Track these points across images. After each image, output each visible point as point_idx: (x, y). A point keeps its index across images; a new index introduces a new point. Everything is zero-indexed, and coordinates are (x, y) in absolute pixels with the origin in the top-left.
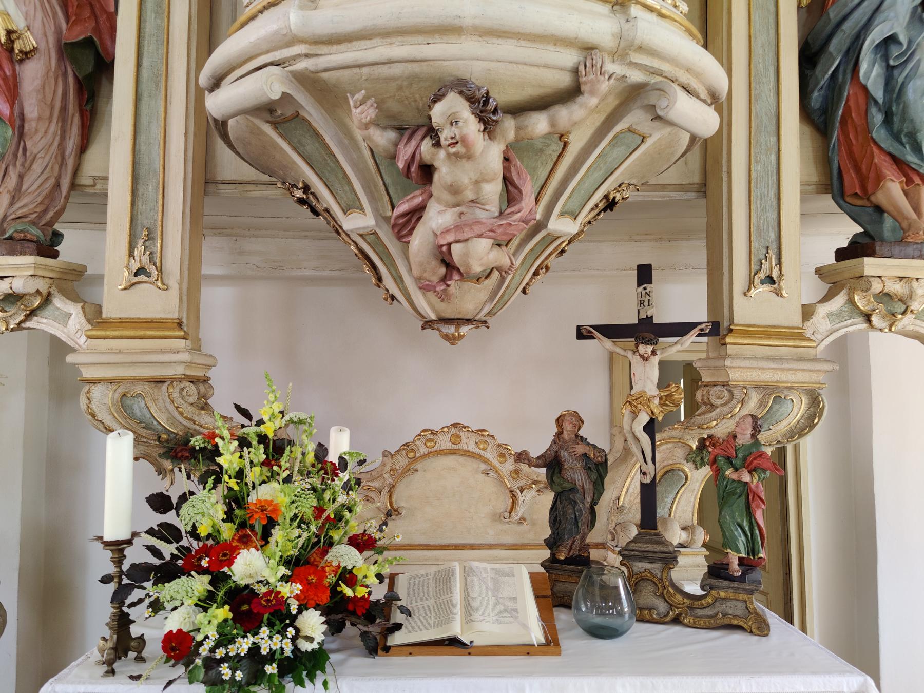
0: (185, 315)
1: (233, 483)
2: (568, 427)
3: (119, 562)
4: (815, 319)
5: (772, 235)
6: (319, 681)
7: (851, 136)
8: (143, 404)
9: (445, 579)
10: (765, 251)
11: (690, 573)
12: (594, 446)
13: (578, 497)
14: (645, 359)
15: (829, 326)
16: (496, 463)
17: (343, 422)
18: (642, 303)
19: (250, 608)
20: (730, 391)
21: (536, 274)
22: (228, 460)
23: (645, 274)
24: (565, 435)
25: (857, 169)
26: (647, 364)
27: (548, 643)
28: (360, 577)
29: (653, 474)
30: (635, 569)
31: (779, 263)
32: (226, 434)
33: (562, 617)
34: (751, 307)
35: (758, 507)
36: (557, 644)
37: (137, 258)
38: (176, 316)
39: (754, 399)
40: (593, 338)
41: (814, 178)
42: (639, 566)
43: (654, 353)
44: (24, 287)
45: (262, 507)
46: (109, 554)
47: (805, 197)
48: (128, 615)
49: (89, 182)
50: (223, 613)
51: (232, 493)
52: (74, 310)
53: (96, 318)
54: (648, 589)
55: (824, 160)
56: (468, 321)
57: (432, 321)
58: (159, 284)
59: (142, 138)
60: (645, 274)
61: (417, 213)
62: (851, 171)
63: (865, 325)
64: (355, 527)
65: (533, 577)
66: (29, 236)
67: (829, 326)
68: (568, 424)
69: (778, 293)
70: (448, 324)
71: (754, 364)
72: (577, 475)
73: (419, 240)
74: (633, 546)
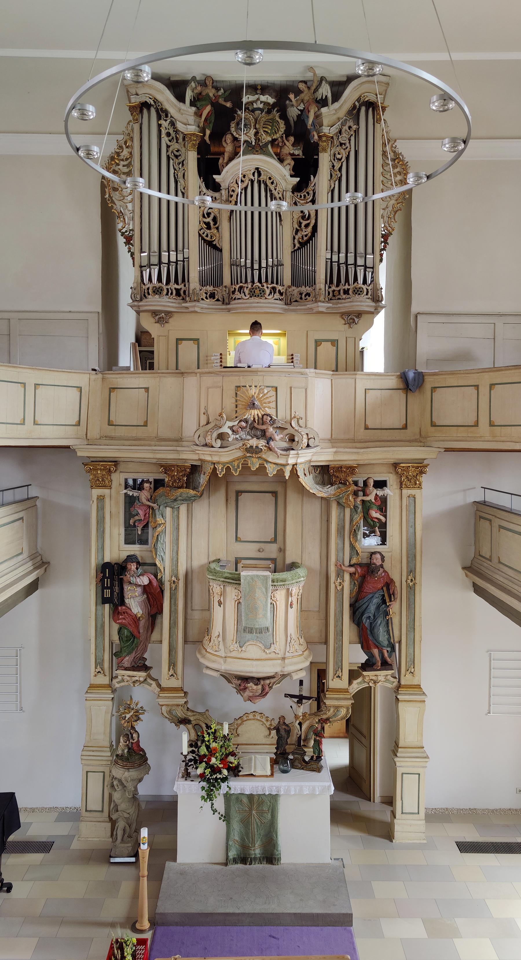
16: (265, 722)
31: (342, 672)
39: (332, 710)
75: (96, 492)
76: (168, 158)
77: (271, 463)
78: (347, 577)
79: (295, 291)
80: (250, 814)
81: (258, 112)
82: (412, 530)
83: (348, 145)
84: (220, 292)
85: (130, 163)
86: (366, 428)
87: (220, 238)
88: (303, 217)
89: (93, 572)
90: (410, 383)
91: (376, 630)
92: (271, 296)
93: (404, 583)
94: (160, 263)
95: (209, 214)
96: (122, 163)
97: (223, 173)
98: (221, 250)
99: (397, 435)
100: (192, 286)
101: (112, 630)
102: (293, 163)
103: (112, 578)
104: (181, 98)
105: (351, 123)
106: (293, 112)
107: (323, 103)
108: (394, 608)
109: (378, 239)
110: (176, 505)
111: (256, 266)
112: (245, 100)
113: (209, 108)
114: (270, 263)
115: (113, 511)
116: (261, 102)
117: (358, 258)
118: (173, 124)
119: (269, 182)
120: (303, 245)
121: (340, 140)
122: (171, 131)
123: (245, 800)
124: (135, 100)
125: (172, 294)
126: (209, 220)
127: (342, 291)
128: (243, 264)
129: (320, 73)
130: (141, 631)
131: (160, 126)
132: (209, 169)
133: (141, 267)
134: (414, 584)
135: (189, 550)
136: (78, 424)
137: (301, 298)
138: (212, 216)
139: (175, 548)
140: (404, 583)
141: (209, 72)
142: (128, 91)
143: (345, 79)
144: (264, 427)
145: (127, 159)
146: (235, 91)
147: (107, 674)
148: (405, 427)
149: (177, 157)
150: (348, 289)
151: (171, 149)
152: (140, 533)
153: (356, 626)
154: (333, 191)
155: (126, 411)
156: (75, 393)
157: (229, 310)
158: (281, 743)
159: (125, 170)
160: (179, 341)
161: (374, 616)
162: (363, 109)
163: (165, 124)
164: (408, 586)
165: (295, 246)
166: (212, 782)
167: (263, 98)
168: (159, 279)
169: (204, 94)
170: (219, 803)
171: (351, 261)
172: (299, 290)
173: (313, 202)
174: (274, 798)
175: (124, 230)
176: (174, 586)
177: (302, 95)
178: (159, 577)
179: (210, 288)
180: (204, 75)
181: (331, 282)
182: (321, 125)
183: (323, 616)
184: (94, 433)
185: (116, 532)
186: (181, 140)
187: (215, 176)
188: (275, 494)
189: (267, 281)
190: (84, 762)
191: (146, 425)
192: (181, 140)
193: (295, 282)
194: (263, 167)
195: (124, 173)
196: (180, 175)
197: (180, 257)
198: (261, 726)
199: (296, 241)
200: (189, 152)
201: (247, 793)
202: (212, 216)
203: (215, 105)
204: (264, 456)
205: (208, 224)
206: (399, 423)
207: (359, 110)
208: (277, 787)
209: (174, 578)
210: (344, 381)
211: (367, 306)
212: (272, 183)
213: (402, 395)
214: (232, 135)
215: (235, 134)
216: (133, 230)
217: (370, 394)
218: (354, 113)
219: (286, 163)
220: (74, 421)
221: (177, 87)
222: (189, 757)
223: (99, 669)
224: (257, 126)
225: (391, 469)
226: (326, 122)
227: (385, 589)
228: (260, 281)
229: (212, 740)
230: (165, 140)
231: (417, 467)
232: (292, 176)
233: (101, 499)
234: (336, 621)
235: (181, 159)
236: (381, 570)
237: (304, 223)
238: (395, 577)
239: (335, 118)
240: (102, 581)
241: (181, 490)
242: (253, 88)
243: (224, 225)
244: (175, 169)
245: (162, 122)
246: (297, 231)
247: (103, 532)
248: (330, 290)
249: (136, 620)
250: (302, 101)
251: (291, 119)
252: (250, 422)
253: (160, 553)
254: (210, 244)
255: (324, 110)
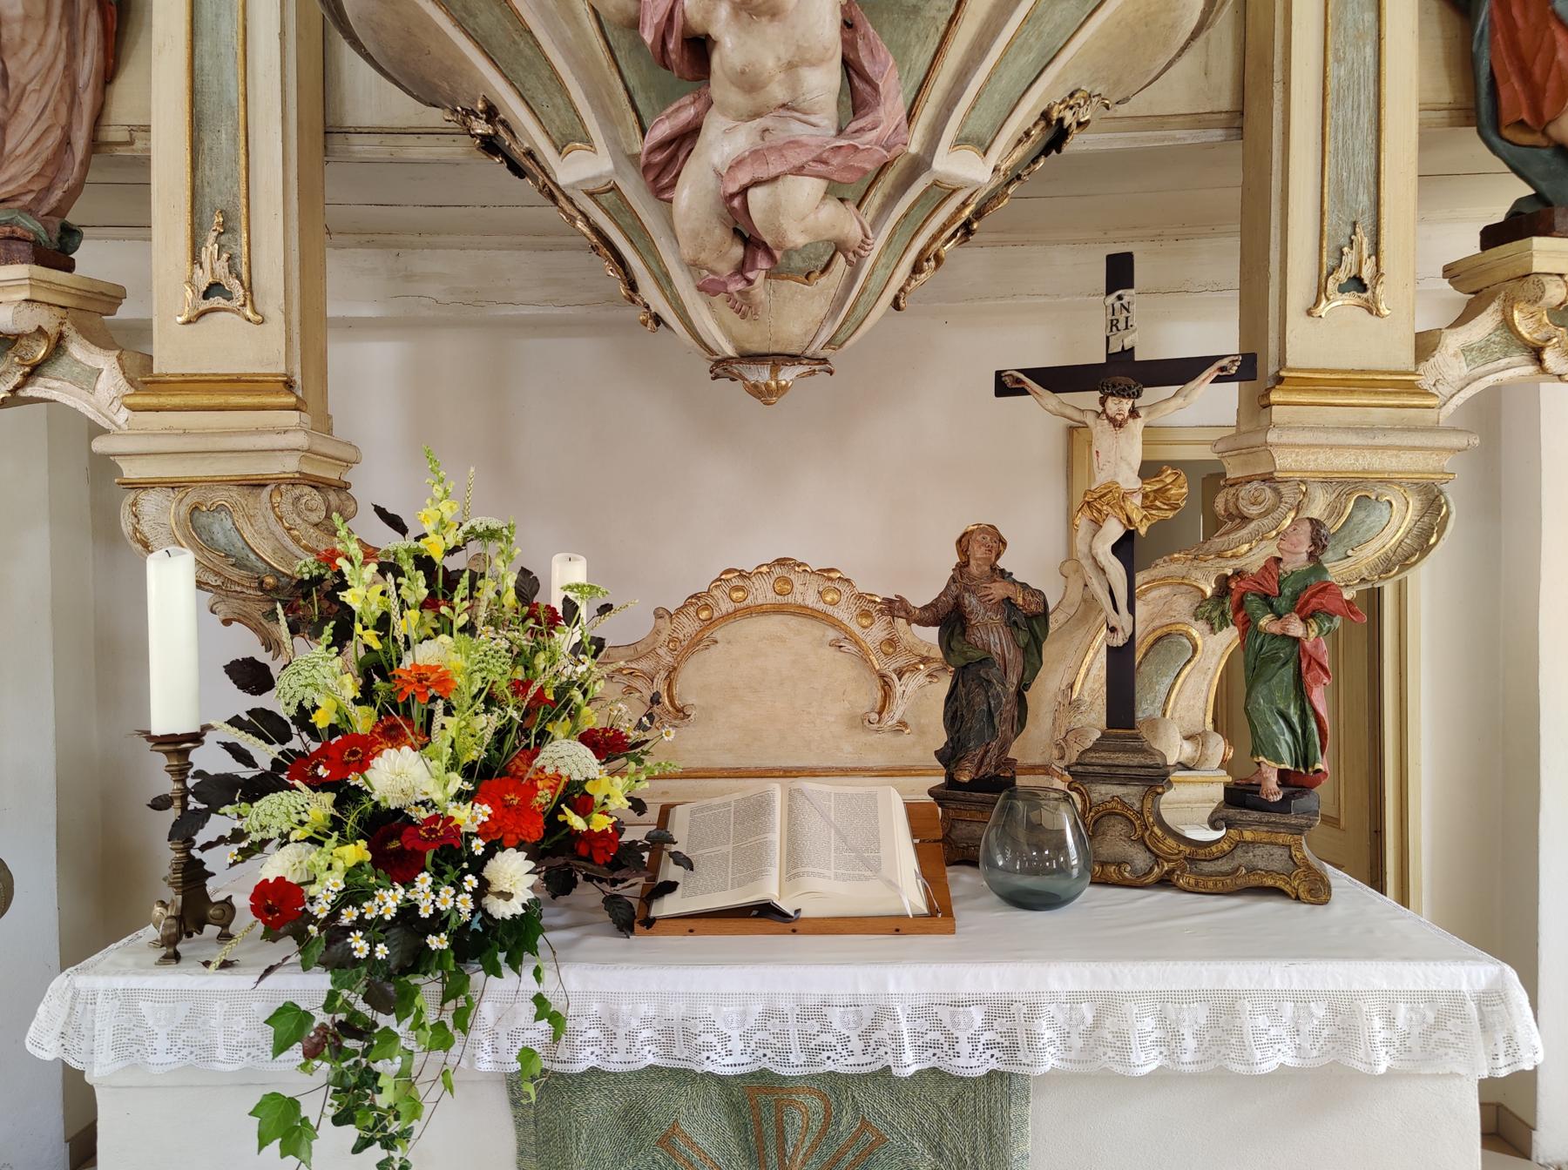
0: (297, 369)
1: (370, 637)
2: (977, 552)
3: (180, 773)
4: (1438, 358)
5: (1365, 200)
6: (527, 971)
7: (1516, 12)
8: (228, 524)
9: (757, 811)
10: (1349, 230)
11: (1191, 807)
12: (1025, 586)
13: (994, 674)
14: (1117, 424)
15: (1465, 371)
16: (854, 627)
17: (573, 547)
18: (1113, 324)
19: (396, 841)
20: (1277, 491)
21: (917, 269)
22: (363, 593)
23: (1120, 272)
24: (973, 568)
25: (1525, 74)
26: (1122, 433)
27: (933, 913)
28: (598, 798)
29: (1129, 632)
30: (1095, 797)
32: (354, 549)
33: (962, 880)
34: (1319, 335)
35: (1317, 681)
36: (948, 914)
37: (207, 265)
38: (282, 369)
40: (1023, 392)
41: (1446, 97)
42: (1103, 792)
43: (1134, 413)
44: (14, 322)
45: (421, 676)
46: (162, 760)
47: (1426, 142)
48: (201, 863)
49: (121, 136)
50: (357, 852)
51: (372, 656)
52: (105, 362)
53: (144, 379)
54: (1117, 828)
55: (1464, 61)
56: (794, 358)
57: (727, 360)
58: (249, 313)
59: (205, 45)
60: (1120, 272)
61: (687, 137)
62: (1514, 79)
63: (1532, 369)
64: (591, 719)
65: (914, 812)
66: (19, 233)
67: (1465, 371)
68: (979, 549)
69: (1372, 309)
71: (1322, 438)
72: (994, 638)
73: (693, 191)
74: (1093, 757)
198: (830, 652)
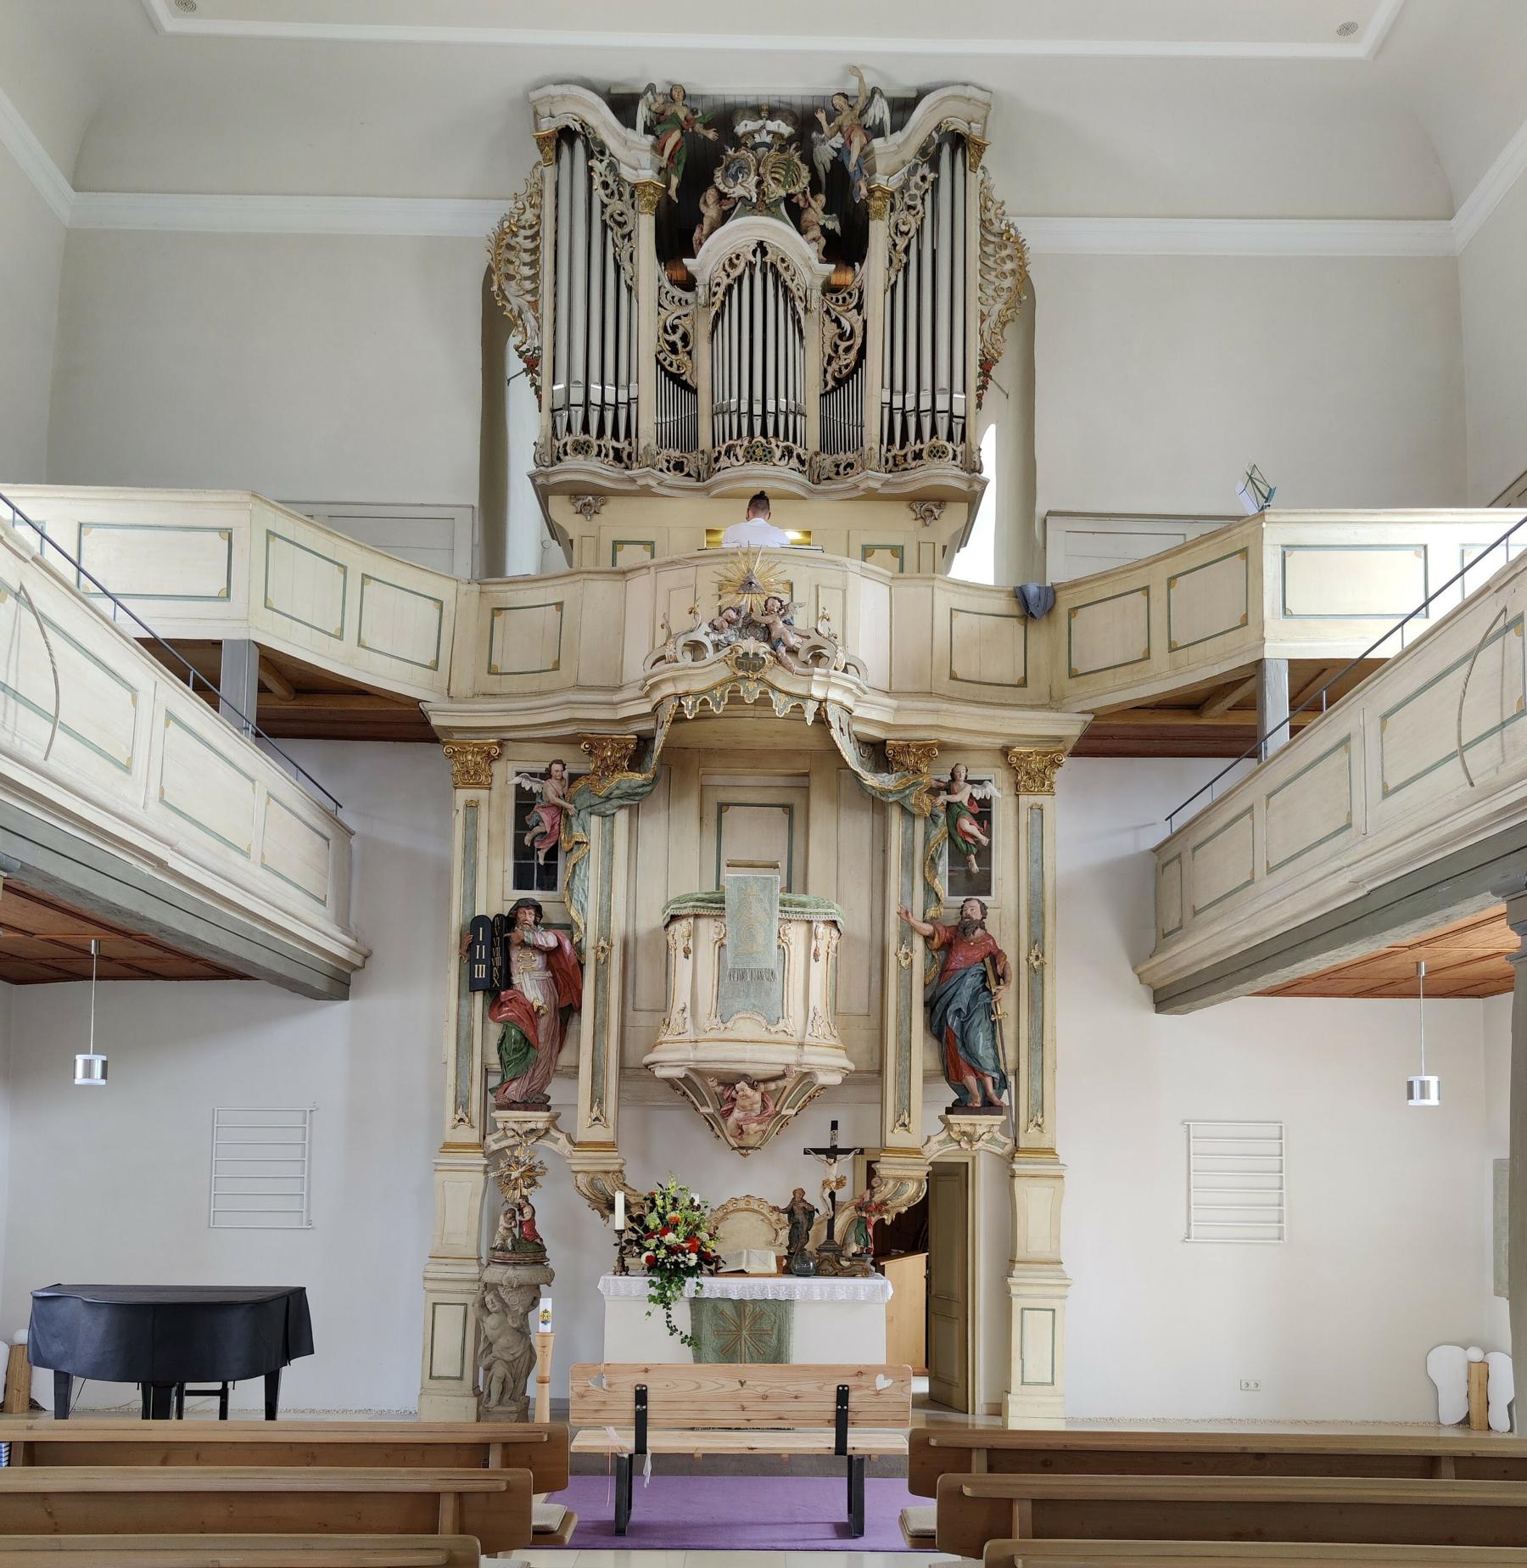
17: (696, 1192)
23: (834, 1125)
39: (891, 1183)
60: (834, 1125)
61: (731, 1111)
68: (799, 1194)
70: (743, 1149)
72: (800, 1217)
73: (731, 1120)
75: (462, 796)
76: (605, 226)
77: (780, 691)
78: (919, 943)
79: (827, 461)
80: (739, 1337)
81: (761, 150)
82: (1036, 868)
83: (920, 207)
84: (692, 461)
85: (537, 233)
86: (953, 677)
87: (695, 370)
88: (841, 336)
89: (455, 938)
90: (1032, 606)
91: (971, 1035)
92: (783, 462)
93: (1024, 963)
94: (587, 403)
95: (674, 328)
96: (523, 233)
97: (702, 253)
98: (695, 392)
99: (1008, 695)
100: (643, 443)
101: (487, 1036)
102: (823, 241)
103: (490, 945)
104: (629, 121)
105: (925, 170)
106: (824, 153)
107: (877, 131)
108: (1006, 1001)
109: (974, 369)
110: (608, 808)
111: (758, 409)
112: (740, 129)
113: (676, 136)
114: (782, 407)
115: (494, 830)
116: (769, 133)
117: (938, 397)
118: (612, 167)
119: (781, 267)
120: (840, 382)
121: (906, 199)
122: (610, 180)
123: (729, 1310)
124: (548, 126)
125: (607, 456)
126: (675, 338)
127: (910, 456)
128: (734, 407)
129: (871, 80)
130: (541, 1040)
131: (590, 169)
132: (676, 241)
133: (553, 411)
134: (1042, 965)
135: (632, 900)
136: (435, 667)
137: (838, 473)
138: (680, 332)
139: (606, 888)
140: (1024, 963)
141: (680, 78)
142: (536, 113)
143: (914, 95)
144: (769, 619)
145: (531, 227)
146: (725, 117)
147: (476, 1124)
148: (1023, 683)
149: (621, 225)
150: (921, 450)
151: (609, 211)
152: (542, 862)
153: (936, 1042)
154: (893, 288)
155: (520, 646)
156: (431, 610)
157: (707, 490)
158: (797, 1236)
159: (529, 245)
160: (617, 544)
161: (968, 1009)
162: (946, 150)
163: (599, 167)
164: (1031, 968)
165: (826, 384)
166: (667, 1272)
167: (772, 126)
168: (586, 428)
169: (668, 113)
170: (682, 1315)
171: (926, 404)
172: (832, 461)
173: (859, 307)
174: (781, 1308)
175: (523, 348)
176: (602, 956)
177: (839, 119)
178: (576, 939)
179: (675, 454)
180: (668, 83)
181: (891, 441)
182: (872, 171)
183: (875, 1022)
184: (462, 686)
185: (497, 866)
186: (627, 196)
187: (686, 261)
188: (788, 808)
189: (776, 434)
190: (429, 1285)
191: (556, 667)
192: (627, 196)
193: (824, 447)
194: (771, 240)
195: (526, 251)
196: (625, 255)
197: (623, 397)
199: (829, 377)
200: (642, 217)
201: (735, 1297)
202: (680, 332)
203: (689, 138)
204: (767, 677)
205: (673, 345)
206: (1014, 676)
207: (939, 147)
208: (788, 1287)
209: (602, 943)
210: (912, 592)
211: (956, 477)
212: (787, 268)
213: (1016, 627)
214: (718, 190)
215: (721, 187)
216: (539, 348)
217: (960, 619)
218: (929, 156)
219: (811, 235)
220: (429, 659)
221: (623, 105)
222: (625, 1236)
223: (461, 1114)
224: (761, 170)
225: (999, 760)
226: (881, 165)
227: (987, 960)
228: (764, 433)
229: (669, 1208)
230: (599, 194)
231: (1046, 754)
232: (821, 262)
233: (472, 806)
234: (899, 1025)
235: (626, 230)
236: (979, 932)
237: (843, 345)
238: (1007, 946)
239: (897, 159)
240: (470, 949)
241: (618, 776)
242: (756, 111)
243: (702, 348)
244: (615, 245)
245: (593, 163)
246: (830, 360)
247: (475, 865)
248: (890, 455)
249: (533, 1014)
250: (840, 129)
251: (820, 168)
252: (743, 614)
253: (578, 895)
254: (675, 378)
255: (877, 143)
